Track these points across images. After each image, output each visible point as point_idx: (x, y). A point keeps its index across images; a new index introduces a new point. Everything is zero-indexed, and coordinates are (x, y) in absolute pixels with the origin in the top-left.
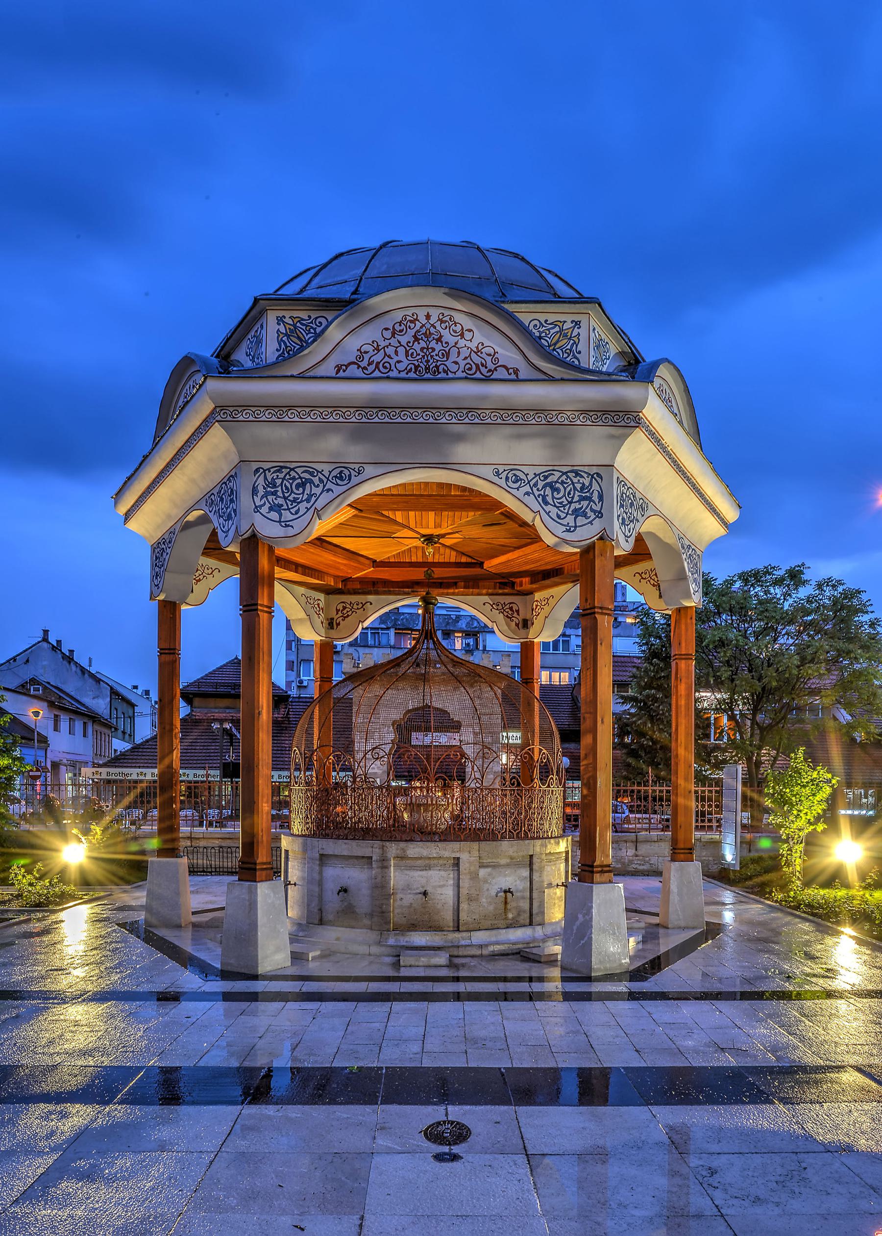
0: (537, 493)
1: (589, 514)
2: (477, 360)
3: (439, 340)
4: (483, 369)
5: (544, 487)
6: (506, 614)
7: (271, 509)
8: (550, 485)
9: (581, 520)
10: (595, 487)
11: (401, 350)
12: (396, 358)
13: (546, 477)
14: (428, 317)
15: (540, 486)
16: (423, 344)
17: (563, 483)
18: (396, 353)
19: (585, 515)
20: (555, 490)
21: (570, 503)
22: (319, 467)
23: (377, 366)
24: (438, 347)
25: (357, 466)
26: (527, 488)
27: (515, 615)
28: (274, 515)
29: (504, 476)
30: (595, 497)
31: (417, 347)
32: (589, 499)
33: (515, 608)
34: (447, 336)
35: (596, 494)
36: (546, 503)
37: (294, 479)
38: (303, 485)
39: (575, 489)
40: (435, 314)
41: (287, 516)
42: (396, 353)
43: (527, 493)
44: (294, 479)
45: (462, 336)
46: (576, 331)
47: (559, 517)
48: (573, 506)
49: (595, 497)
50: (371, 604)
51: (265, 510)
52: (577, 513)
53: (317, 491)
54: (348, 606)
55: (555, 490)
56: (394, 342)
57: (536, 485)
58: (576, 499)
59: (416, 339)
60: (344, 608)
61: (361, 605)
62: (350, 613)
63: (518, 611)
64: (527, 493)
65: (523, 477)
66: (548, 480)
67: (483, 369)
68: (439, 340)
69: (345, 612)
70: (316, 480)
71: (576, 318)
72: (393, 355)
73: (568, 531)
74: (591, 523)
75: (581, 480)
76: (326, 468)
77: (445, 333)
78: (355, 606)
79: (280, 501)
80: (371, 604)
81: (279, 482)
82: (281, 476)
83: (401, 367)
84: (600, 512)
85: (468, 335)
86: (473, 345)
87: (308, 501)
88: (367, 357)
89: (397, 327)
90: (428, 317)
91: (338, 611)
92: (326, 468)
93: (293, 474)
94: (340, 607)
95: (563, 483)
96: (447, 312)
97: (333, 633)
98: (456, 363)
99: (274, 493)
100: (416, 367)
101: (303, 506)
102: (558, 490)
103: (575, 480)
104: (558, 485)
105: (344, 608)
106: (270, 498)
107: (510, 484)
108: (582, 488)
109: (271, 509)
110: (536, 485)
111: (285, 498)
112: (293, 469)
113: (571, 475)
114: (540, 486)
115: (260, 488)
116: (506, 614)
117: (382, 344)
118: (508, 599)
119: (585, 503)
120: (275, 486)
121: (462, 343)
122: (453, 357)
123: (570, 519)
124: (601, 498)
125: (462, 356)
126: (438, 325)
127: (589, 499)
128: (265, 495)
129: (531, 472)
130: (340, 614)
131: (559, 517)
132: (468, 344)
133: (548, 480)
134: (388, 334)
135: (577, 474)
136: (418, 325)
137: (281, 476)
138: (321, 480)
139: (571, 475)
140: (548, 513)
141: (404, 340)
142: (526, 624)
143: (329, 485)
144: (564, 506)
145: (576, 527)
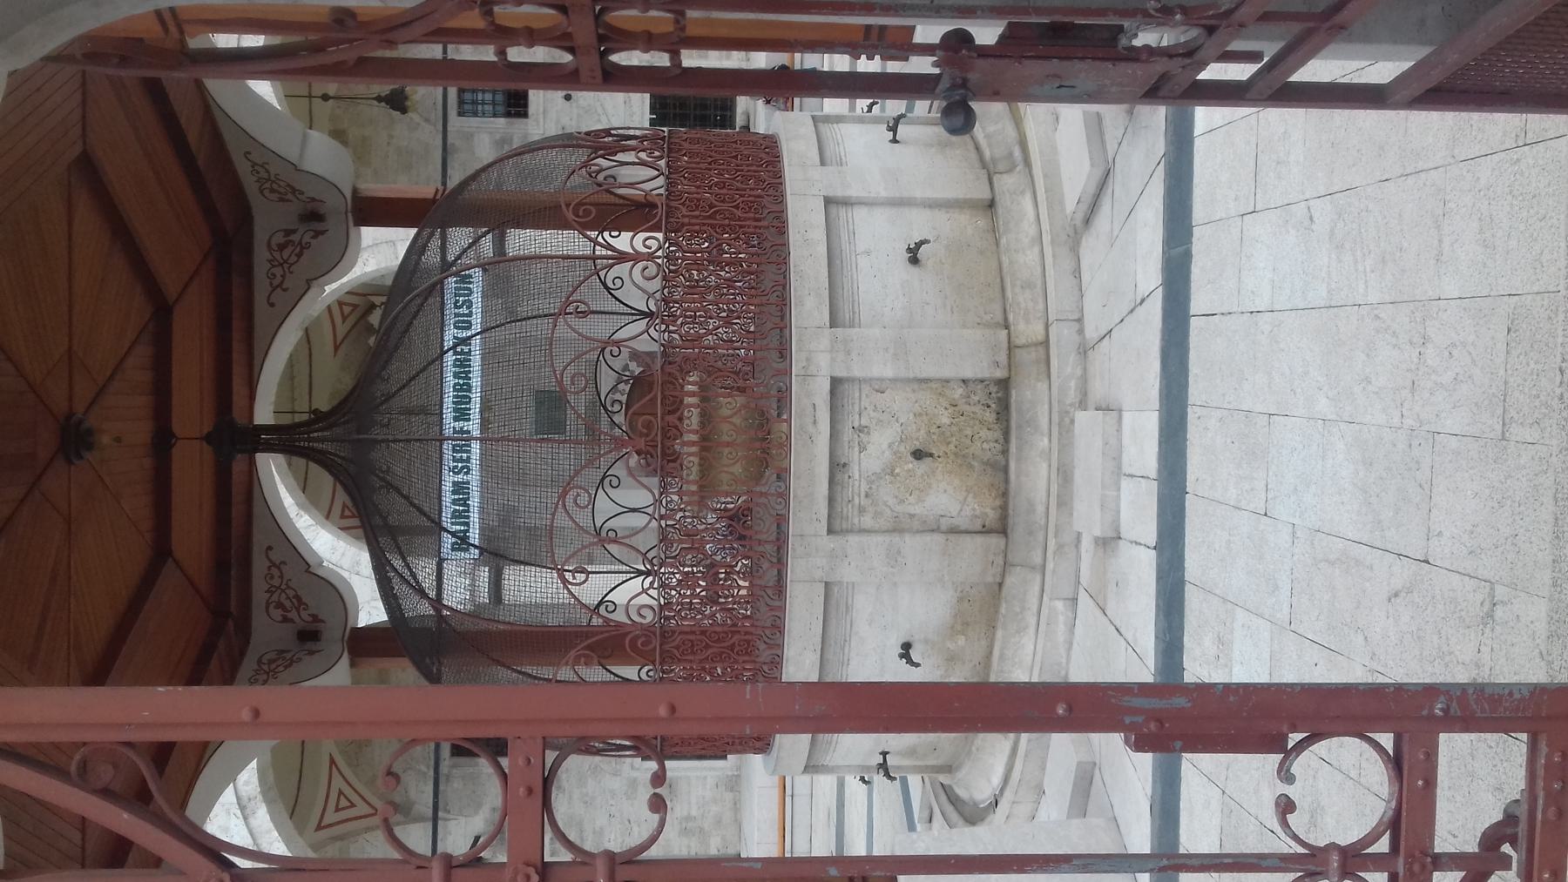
6: (294, 258)
27: (295, 237)
33: (279, 238)
50: (270, 548)
54: (275, 597)
60: (280, 605)
61: (275, 571)
62: (291, 593)
69: (288, 604)
78: (276, 582)
80: (270, 548)
91: (285, 620)
94: (277, 614)
97: (332, 634)
105: (280, 605)
116: (294, 258)
118: (261, 256)
130: (293, 615)
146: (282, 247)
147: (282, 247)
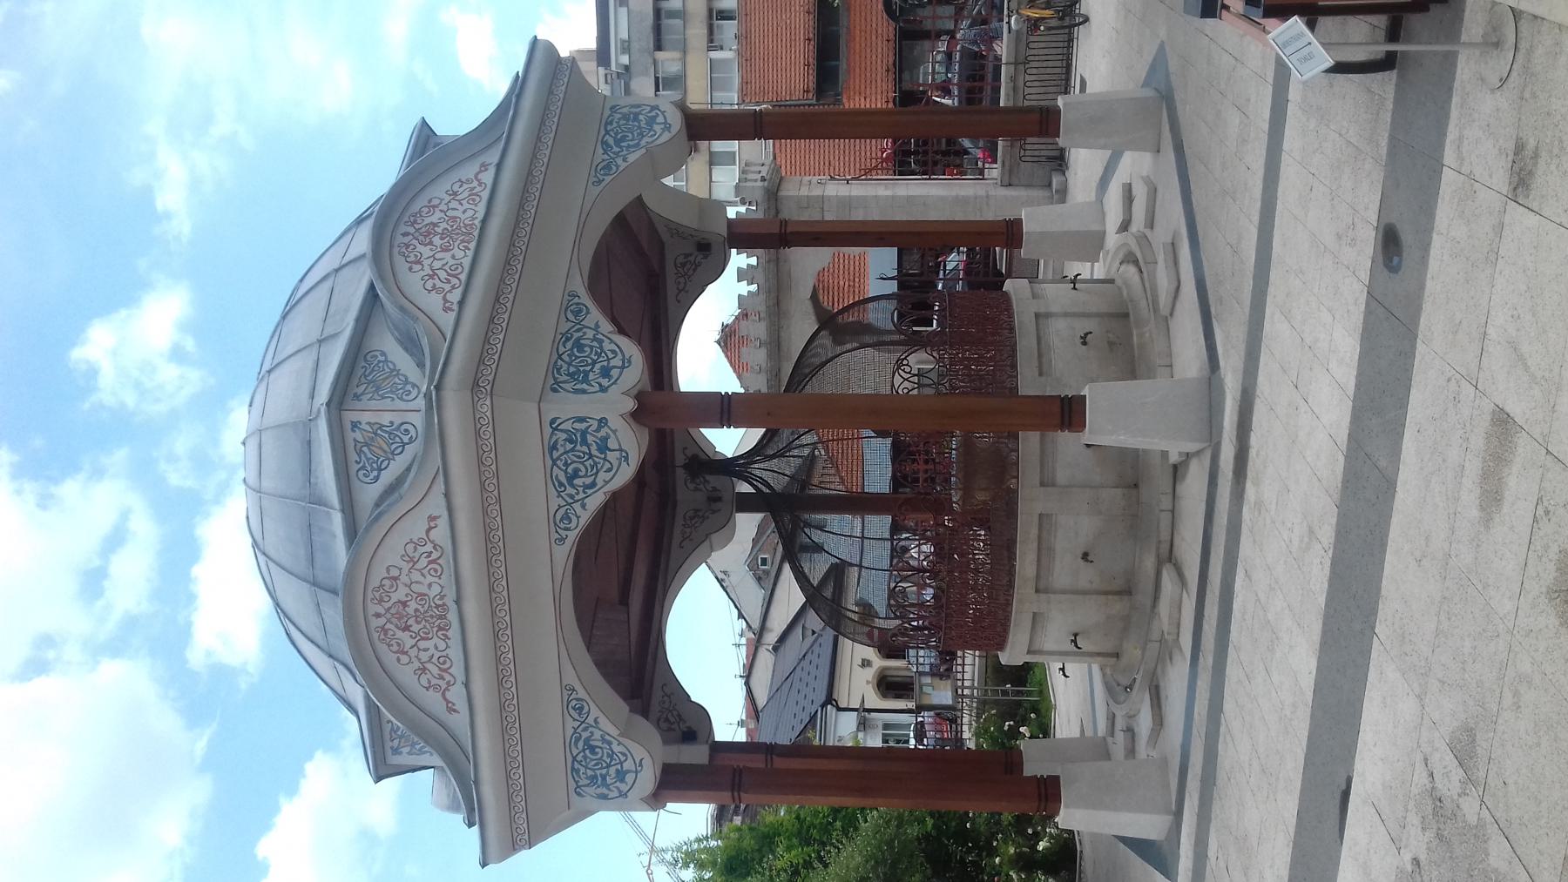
0: (582, 495)
1: (603, 433)
2: (423, 562)
3: (404, 604)
4: (434, 556)
5: (573, 486)
7: (622, 780)
8: (570, 479)
9: (612, 444)
10: (567, 426)
11: (422, 644)
12: (432, 650)
13: (561, 484)
14: (378, 615)
15: (573, 492)
16: (411, 622)
17: (566, 464)
18: (426, 650)
19: (605, 439)
20: (576, 474)
21: (591, 456)
22: (570, 732)
23: (445, 670)
24: (413, 605)
25: (566, 693)
26: (577, 506)
27: (692, 259)
28: (629, 778)
29: (564, 533)
30: (583, 426)
31: (415, 628)
32: (584, 433)
33: (681, 259)
34: (401, 594)
35: (577, 426)
36: (593, 484)
37: (585, 757)
38: (592, 749)
39: (572, 450)
40: (373, 608)
41: (628, 765)
42: (426, 650)
43: (583, 506)
44: (585, 757)
45: (395, 579)
46: (364, 426)
47: (609, 470)
48: (594, 452)
49: (583, 426)
51: (624, 788)
52: (603, 448)
53: (597, 734)
55: (576, 474)
56: (413, 652)
57: (572, 497)
58: (585, 449)
59: (407, 628)
63: (687, 256)
64: (583, 506)
65: (562, 511)
66: (564, 480)
67: (434, 556)
68: (404, 604)
70: (585, 735)
71: (348, 426)
72: (429, 653)
73: (626, 459)
74: (614, 432)
75: (561, 442)
76: (570, 724)
77: (395, 597)
79: (612, 771)
81: (590, 773)
82: (582, 770)
83: (442, 645)
84: (600, 421)
85: (394, 573)
86: (406, 567)
87: (610, 743)
88: (434, 682)
89: (395, 648)
90: (378, 615)
91: (696, 489)
92: (570, 724)
93: (579, 758)
95: (566, 464)
96: (370, 596)
98: (430, 585)
99: (604, 778)
100: (440, 629)
101: (616, 748)
102: (576, 471)
103: (561, 450)
104: (570, 470)
106: (609, 781)
107: (573, 525)
108: (571, 441)
109: (622, 780)
110: (572, 497)
111: (609, 766)
112: (574, 758)
113: (556, 454)
114: (573, 492)
115: (600, 791)
117: (417, 665)
119: (590, 439)
120: (595, 777)
121: (404, 578)
122: (424, 589)
123: (611, 456)
124: (582, 420)
125: (421, 579)
126: (387, 605)
127: (584, 433)
128: (607, 786)
129: (555, 502)
131: (609, 470)
132: (405, 571)
133: (564, 480)
134: (405, 659)
135: (554, 447)
136: (389, 626)
137: (582, 770)
138: (585, 729)
139: (556, 454)
140: (607, 482)
141: (410, 642)
142: (704, 247)
143: (590, 720)
144: (596, 463)
145: (621, 450)
146: (683, 265)
147: (683, 265)
